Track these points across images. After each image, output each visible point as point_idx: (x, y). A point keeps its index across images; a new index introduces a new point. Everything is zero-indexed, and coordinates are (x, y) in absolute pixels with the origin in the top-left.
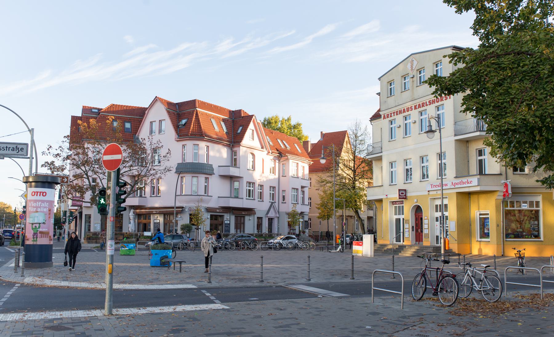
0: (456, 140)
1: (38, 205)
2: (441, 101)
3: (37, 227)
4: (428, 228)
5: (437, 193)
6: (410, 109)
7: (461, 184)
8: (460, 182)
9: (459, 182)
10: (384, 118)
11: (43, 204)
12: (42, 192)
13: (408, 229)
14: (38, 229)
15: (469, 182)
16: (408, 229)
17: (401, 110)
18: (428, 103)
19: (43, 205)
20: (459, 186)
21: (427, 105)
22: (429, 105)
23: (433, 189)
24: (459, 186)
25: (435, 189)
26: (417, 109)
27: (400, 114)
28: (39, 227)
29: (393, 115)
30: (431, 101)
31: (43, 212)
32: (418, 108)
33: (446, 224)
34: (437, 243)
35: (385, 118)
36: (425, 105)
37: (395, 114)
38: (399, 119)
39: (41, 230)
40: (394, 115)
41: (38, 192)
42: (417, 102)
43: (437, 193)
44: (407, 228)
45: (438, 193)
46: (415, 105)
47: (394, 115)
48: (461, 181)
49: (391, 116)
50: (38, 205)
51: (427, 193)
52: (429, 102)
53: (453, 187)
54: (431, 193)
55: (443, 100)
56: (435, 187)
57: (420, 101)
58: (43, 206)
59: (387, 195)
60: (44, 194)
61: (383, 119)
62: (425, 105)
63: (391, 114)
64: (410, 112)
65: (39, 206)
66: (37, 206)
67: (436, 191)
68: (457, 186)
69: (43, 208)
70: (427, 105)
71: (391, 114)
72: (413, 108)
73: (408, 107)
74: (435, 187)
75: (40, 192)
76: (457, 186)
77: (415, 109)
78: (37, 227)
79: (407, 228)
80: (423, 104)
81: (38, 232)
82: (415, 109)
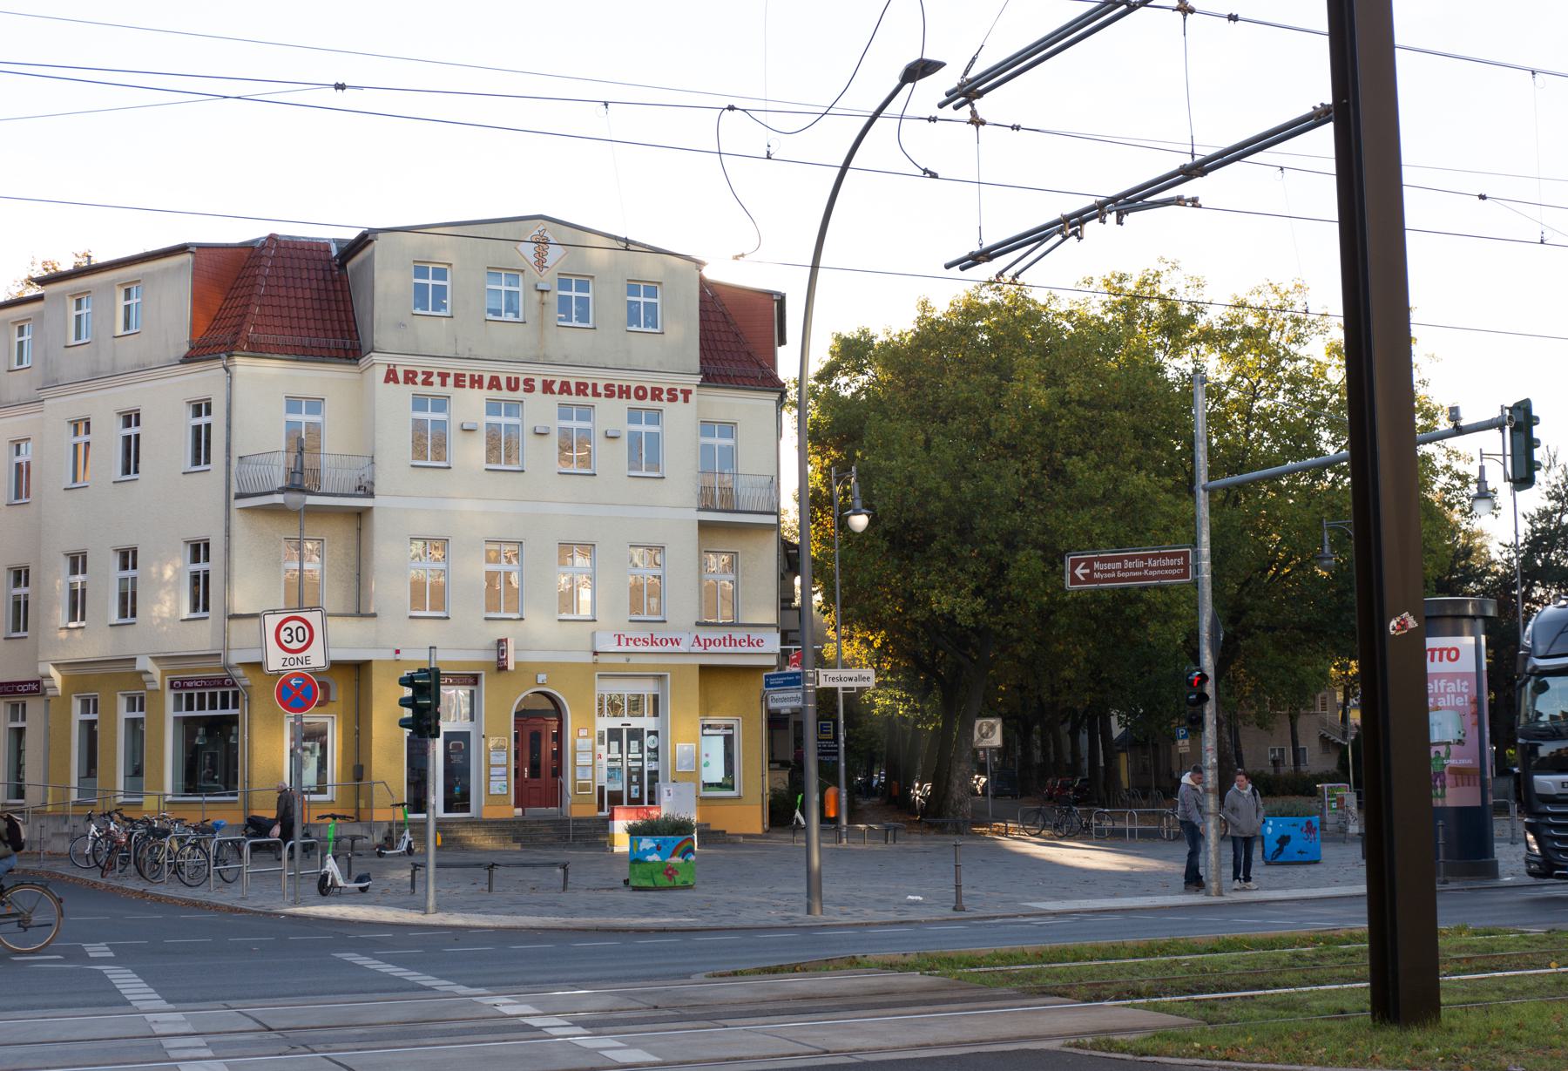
0: (700, 522)
1: (1439, 687)
2: (653, 399)
3: (1443, 755)
4: (489, 766)
5: (628, 660)
6: (522, 386)
7: (727, 642)
8: (724, 639)
9: (721, 638)
10: (391, 376)
11: (1453, 684)
12: (1445, 649)
13: (504, 769)
14: (1445, 762)
15: (755, 643)
16: (504, 769)
17: (481, 377)
18: (600, 389)
19: (1452, 687)
20: (722, 649)
21: (596, 394)
22: (606, 396)
23: (624, 648)
24: (722, 649)
25: (632, 648)
26: (553, 392)
27: (472, 386)
28: (1448, 755)
29: (436, 379)
30: (616, 389)
31: (1455, 708)
32: (561, 392)
33: (628, 752)
34: (601, 808)
35: (396, 381)
36: (589, 391)
37: (450, 381)
38: (470, 405)
39: (1452, 762)
40: (444, 384)
41: (1435, 649)
42: (558, 375)
43: (628, 660)
44: (499, 766)
45: (632, 661)
46: (549, 379)
47: (444, 384)
48: (728, 637)
49: (426, 382)
50: (1439, 687)
51: (589, 658)
52: (607, 387)
53: (701, 649)
54: (602, 659)
55: (661, 400)
56: (631, 643)
57: (574, 376)
58: (1454, 690)
59: (398, 652)
60: (1453, 654)
61: (387, 380)
62: (589, 391)
63: (429, 374)
64: (520, 394)
65: (1442, 691)
66: (1436, 691)
67: (625, 656)
68: (711, 649)
69: (1453, 696)
70: (599, 395)
71: (429, 374)
72: (538, 385)
73: (513, 376)
74: (631, 643)
75: (1441, 650)
76: (711, 649)
77: (544, 392)
78: (1443, 755)
79: (499, 766)
80: (581, 389)
81: (1446, 770)
82: (544, 392)
